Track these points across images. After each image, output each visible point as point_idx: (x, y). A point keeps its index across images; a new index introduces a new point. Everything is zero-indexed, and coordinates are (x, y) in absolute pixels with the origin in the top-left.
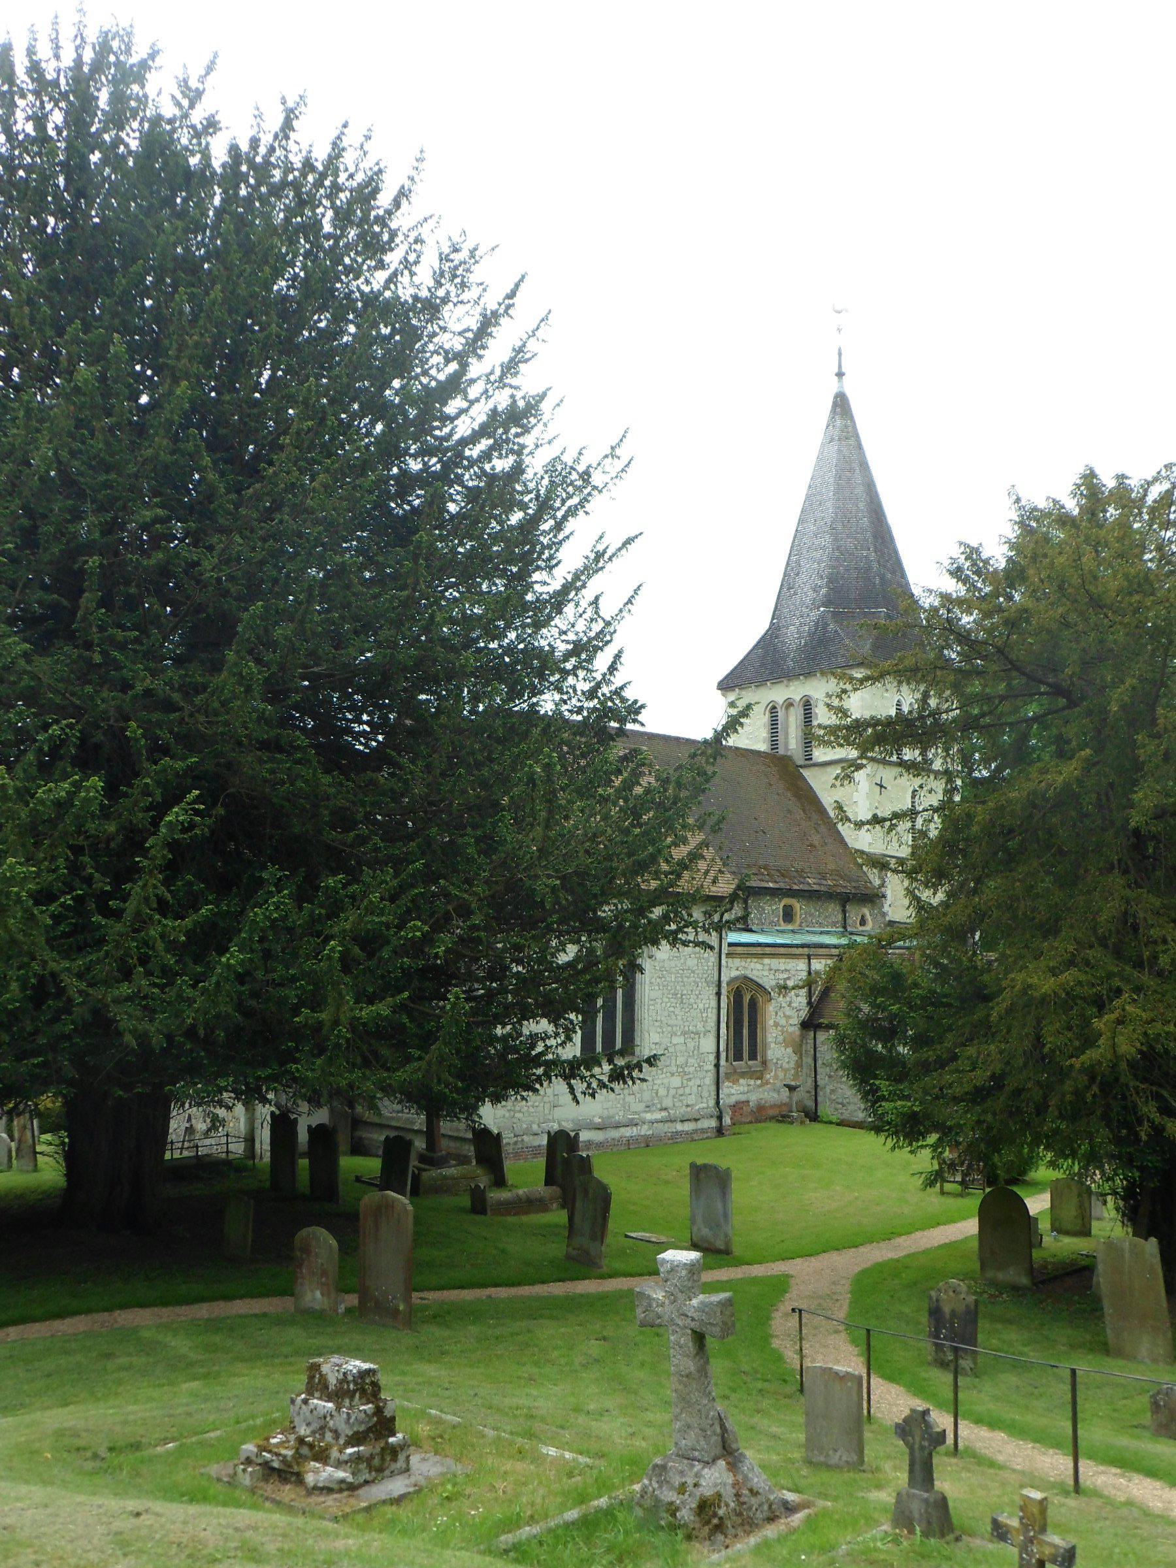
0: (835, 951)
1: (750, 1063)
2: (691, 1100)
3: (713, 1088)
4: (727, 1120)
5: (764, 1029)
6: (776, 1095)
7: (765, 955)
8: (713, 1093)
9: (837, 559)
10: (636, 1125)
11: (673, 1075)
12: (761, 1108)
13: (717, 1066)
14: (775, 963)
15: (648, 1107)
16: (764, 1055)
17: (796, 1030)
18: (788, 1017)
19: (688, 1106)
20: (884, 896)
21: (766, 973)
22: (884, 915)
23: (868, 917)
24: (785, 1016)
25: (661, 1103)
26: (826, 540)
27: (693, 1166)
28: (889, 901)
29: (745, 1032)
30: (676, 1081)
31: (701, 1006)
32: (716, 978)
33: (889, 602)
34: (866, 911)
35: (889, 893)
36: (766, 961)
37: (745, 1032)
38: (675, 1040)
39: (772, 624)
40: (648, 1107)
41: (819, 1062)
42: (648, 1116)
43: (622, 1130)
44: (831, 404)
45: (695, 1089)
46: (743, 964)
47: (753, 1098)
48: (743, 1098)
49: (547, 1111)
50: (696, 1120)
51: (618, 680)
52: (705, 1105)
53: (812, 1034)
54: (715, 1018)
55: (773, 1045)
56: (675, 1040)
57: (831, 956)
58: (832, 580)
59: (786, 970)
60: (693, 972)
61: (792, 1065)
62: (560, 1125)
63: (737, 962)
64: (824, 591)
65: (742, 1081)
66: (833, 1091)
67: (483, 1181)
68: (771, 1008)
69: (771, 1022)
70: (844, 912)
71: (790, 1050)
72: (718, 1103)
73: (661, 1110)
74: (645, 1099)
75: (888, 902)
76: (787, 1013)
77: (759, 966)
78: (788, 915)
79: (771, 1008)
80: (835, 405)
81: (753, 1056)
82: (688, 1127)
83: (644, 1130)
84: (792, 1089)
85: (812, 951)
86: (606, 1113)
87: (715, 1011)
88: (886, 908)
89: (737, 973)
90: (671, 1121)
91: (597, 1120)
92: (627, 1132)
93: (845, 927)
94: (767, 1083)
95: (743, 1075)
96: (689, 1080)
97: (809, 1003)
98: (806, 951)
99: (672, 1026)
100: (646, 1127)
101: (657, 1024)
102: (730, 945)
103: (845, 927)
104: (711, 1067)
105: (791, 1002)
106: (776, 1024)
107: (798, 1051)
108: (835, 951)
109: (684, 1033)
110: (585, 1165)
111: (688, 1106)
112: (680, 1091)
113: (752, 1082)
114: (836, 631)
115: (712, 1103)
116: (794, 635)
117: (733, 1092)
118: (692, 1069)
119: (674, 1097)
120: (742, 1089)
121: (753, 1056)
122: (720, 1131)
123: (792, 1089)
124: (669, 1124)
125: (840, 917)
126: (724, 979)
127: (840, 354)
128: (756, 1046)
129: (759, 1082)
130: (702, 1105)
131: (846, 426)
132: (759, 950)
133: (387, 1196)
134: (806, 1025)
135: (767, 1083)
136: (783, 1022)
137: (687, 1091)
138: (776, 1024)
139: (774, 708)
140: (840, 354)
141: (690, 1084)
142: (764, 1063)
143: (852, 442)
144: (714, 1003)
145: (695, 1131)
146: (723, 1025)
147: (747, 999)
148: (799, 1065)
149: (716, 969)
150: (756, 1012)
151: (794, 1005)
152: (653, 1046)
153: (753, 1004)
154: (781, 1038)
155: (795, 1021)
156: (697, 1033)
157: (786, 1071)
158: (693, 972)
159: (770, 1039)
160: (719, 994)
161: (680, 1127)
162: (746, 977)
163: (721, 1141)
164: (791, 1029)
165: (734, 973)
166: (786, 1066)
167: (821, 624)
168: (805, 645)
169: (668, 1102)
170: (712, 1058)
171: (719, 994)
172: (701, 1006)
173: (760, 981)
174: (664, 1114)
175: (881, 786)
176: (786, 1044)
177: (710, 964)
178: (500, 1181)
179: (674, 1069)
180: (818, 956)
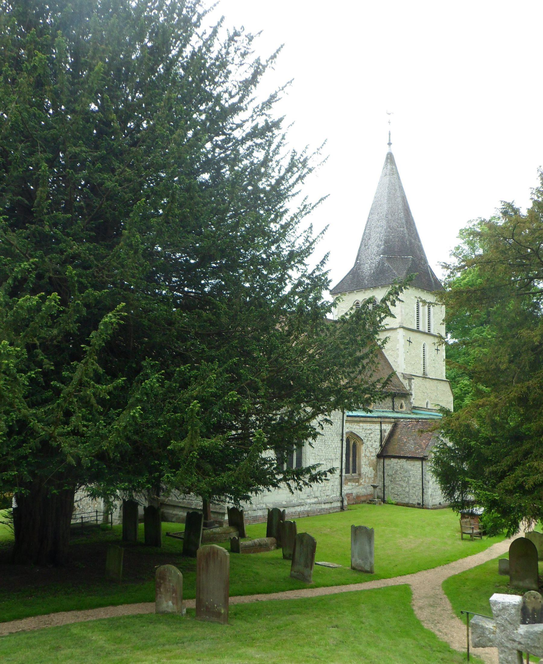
0: (393, 420)
1: (353, 474)
2: (329, 493)
3: (339, 487)
4: (345, 503)
5: (360, 458)
6: (365, 491)
8: (339, 489)
9: (389, 232)
10: (303, 505)
12: (358, 497)
13: (341, 476)
14: (365, 425)
16: (360, 471)
17: (374, 458)
18: (372, 452)
19: (327, 496)
20: (411, 395)
21: (361, 430)
22: (411, 403)
23: (404, 404)
24: (369, 451)
25: (314, 494)
26: (384, 223)
27: (353, 527)
28: (413, 397)
29: (351, 459)
31: (334, 446)
33: (413, 253)
34: (403, 402)
35: (413, 393)
36: (361, 424)
37: (351, 459)
39: (356, 263)
40: (308, 496)
41: (386, 475)
42: (309, 501)
43: (296, 508)
44: (385, 157)
45: (330, 487)
46: (350, 426)
47: (355, 492)
48: (350, 492)
49: (260, 499)
51: (324, 269)
52: (335, 495)
53: (382, 460)
54: (340, 452)
55: (364, 466)
57: (391, 422)
58: (386, 242)
59: (370, 429)
61: (373, 475)
62: (266, 505)
64: (382, 247)
65: (349, 483)
66: (392, 488)
67: (234, 534)
68: (363, 448)
69: (363, 455)
70: (393, 402)
71: (371, 468)
72: (341, 494)
73: (315, 497)
74: (307, 492)
75: (413, 398)
76: (371, 450)
79: (363, 448)
80: (387, 158)
81: (354, 471)
82: (327, 506)
83: (307, 508)
84: (375, 487)
85: (382, 420)
86: (288, 500)
87: (340, 449)
88: (412, 400)
90: (320, 503)
91: (284, 503)
92: (298, 509)
93: (393, 409)
94: (361, 484)
95: (350, 480)
97: (381, 445)
98: (379, 420)
99: (320, 456)
100: (307, 506)
101: (313, 455)
102: (348, 416)
103: (393, 409)
105: (372, 445)
106: (365, 456)
107: (375, 469)
108: (393, 420)
109: (326, 460)
110: (292, 526)
111: (327, 496)
112: (324, 488)
113: (354, 484)
114: (389, 266)
115: (338, 494)
116: (367, 268)
117: (347, 489)
119: (321, 491)
121: (354, 471)
122: (342, 508)
123: (375, 487)
124: (319, 505)
125: (391, 404)
126: (344, 432)
127: (390, 134)
128: (355, 466)
129: (357, 484)
131: (392, 169)
132: (358, 419)
133: (214, 548)
134: (379, 456)
135: (361, 484)
136: (368, 454)
137: (327, 488)
138: (365, 456)
139: (358, 303)
140: (390, 134)
142: (360, 475)
143: (395, 176)
144: (340, 445)
145: (330, 508)
146: (344, 456)
148: (376, 476)
149: (341, 427)
150: (356, 449)
151: (374, 446)
153: (355, 446)
154: (367, 462)
155: (374, 454)
156: (332, 460)
157: (370, 478)
159: (362, 463)
160: (342, 440)
161: (323, 506)
162: (352, 432)
163: (345, 513)
164: (372, 458)
165: (347, 430)
166: (369, 476)
167: (381, 263)
168: (374, 273)
169: (318, 494)
171: (342, 440)
172: (334, 446)
173: (358, 435)
174: (316, 500)
175: (410, 342)
176: (370, 465)
177: (338, 425)
178: (242, 535)
180: (385, 422)
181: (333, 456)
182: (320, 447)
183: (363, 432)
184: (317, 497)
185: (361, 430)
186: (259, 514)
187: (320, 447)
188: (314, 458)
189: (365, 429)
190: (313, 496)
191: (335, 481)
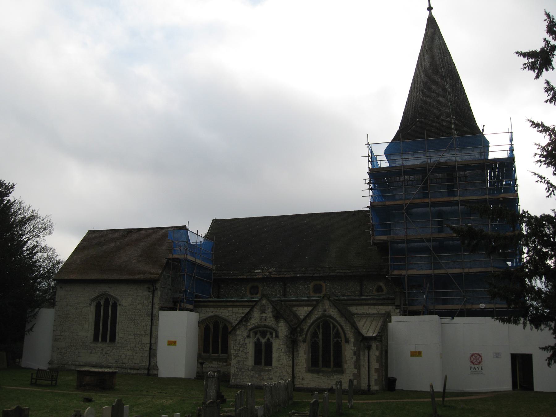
3: (148, 358)
7: (228, 306)
11: (128, 350)
14: (235, 310)
15: (117, 361)
19: (135, 363)
30: (130, 353)
32: (151, 313)
36: (230, 309)
38: (130, 337)
46: (216, 310)
50: (138, 369)
56: (130, 337)
60: (140, 311)
63: (212, 309)
77: (225, 311)
78: (318, 289)
82: (135, 372)
87: (150, 326)
89: (212, 314)
91: (94, 363)
96: (137, 353)
101: (122, 330)
104: (148, 349)
109: (135, 335)
113: (221, 364)
115: (148, 364)
118: (138, 349)
120: (214, 366)
125: (359, 288)
130: (143, 364)
141: (137, 355)
144: (150, 323)
147: (221, 326)
152: (120, 339)
158: (140, 311)
161: (129, 371)
162: (215, 316)
170: (148, 345)
179: (130, 348)
181: (143, 332)
182: (129, 325)
183: (234, 316)
184: (124, 363)
185: (229, 314)
186: (72, 368)
187: (129, 325)
188: (123, 333)
189: (236, 313)
190: (121, 362)
191: (144, 353)
